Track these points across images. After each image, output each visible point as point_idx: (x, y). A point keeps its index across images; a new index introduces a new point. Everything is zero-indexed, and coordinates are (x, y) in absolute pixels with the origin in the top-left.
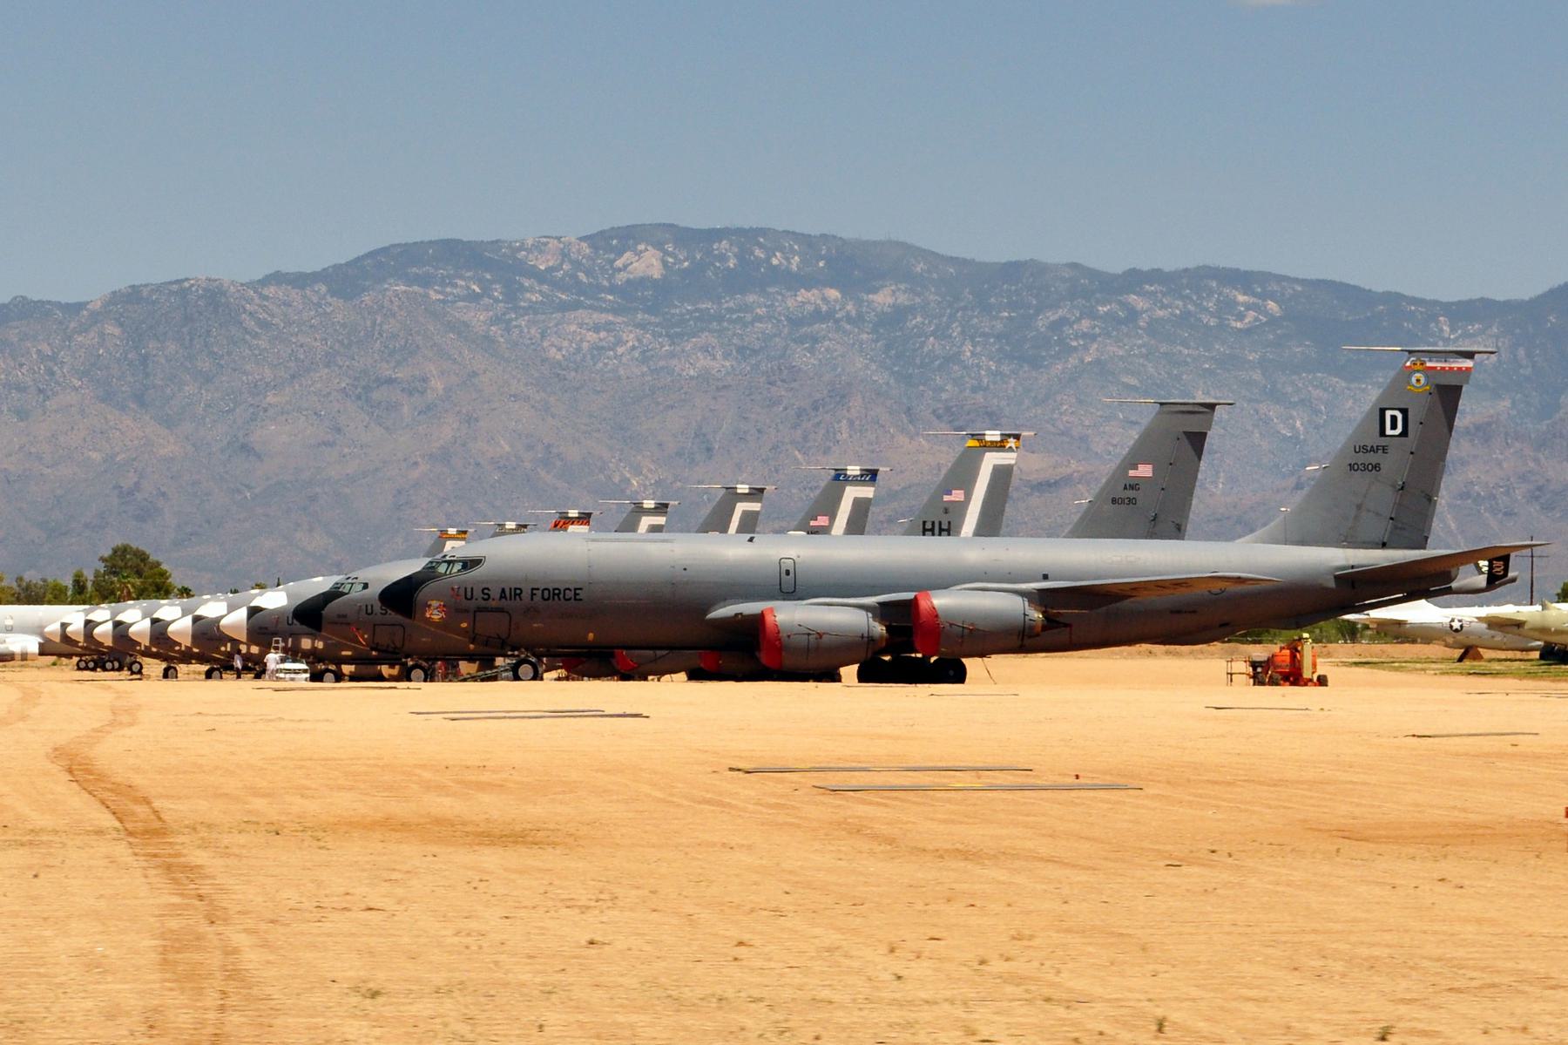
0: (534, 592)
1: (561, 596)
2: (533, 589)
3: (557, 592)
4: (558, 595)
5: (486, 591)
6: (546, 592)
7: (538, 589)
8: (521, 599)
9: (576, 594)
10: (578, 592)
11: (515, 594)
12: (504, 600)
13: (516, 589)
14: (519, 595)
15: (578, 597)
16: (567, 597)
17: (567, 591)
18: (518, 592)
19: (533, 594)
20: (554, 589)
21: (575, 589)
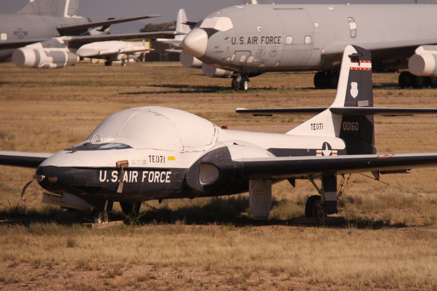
0: (263, 39)
1: (273, 41)
2: (262, 37)
3: (272, 39)
4: (272, 40)
5: (242, 39)
6: (267, 39)
7: (264, 37)
8: (257, 43)
9: (279, 40)
10: (280, 38)
11: (255, 40)
12: (249, 43)
13: (255, 37)
14: (256, 40)
15: (279, 42)
16: (275, 42)
17: (276, 38)
18: (256, 39)
19: (262, 40)
20: (271, 37)
21: (279, 37)
